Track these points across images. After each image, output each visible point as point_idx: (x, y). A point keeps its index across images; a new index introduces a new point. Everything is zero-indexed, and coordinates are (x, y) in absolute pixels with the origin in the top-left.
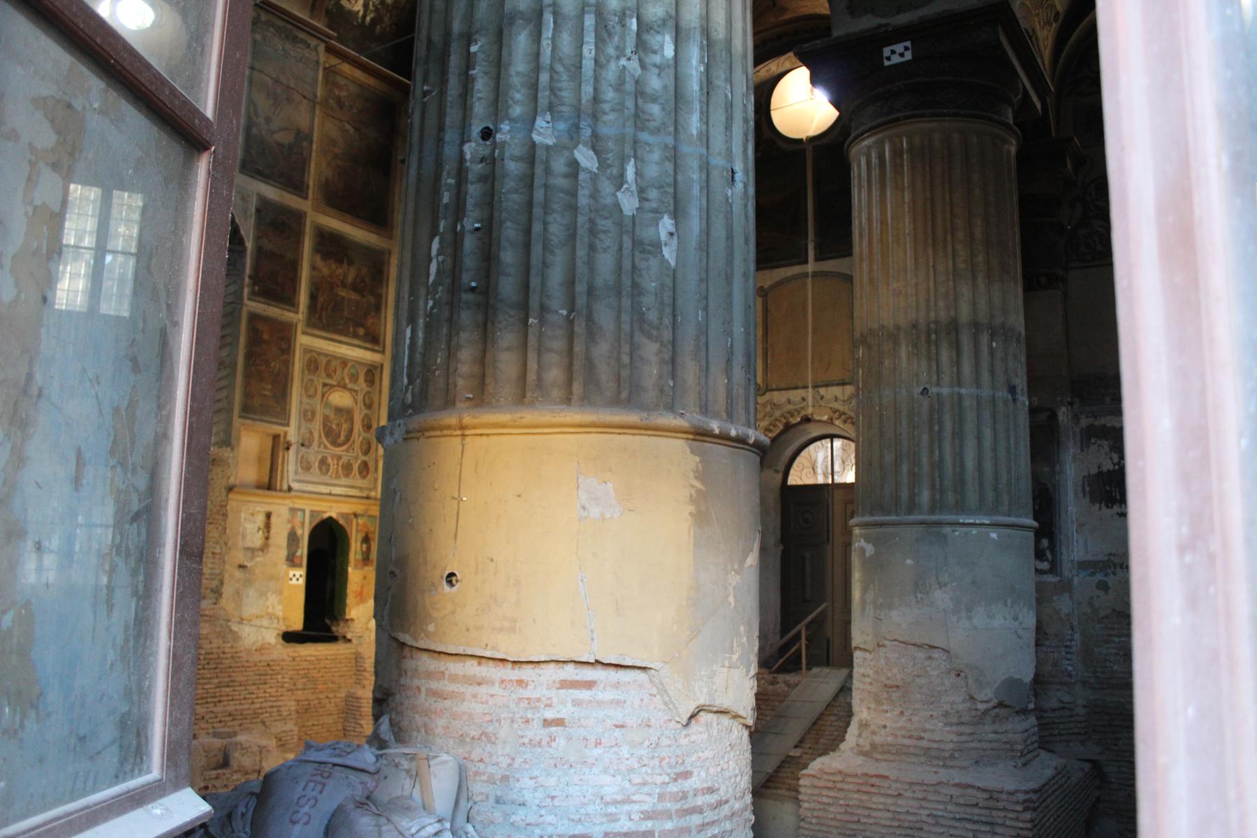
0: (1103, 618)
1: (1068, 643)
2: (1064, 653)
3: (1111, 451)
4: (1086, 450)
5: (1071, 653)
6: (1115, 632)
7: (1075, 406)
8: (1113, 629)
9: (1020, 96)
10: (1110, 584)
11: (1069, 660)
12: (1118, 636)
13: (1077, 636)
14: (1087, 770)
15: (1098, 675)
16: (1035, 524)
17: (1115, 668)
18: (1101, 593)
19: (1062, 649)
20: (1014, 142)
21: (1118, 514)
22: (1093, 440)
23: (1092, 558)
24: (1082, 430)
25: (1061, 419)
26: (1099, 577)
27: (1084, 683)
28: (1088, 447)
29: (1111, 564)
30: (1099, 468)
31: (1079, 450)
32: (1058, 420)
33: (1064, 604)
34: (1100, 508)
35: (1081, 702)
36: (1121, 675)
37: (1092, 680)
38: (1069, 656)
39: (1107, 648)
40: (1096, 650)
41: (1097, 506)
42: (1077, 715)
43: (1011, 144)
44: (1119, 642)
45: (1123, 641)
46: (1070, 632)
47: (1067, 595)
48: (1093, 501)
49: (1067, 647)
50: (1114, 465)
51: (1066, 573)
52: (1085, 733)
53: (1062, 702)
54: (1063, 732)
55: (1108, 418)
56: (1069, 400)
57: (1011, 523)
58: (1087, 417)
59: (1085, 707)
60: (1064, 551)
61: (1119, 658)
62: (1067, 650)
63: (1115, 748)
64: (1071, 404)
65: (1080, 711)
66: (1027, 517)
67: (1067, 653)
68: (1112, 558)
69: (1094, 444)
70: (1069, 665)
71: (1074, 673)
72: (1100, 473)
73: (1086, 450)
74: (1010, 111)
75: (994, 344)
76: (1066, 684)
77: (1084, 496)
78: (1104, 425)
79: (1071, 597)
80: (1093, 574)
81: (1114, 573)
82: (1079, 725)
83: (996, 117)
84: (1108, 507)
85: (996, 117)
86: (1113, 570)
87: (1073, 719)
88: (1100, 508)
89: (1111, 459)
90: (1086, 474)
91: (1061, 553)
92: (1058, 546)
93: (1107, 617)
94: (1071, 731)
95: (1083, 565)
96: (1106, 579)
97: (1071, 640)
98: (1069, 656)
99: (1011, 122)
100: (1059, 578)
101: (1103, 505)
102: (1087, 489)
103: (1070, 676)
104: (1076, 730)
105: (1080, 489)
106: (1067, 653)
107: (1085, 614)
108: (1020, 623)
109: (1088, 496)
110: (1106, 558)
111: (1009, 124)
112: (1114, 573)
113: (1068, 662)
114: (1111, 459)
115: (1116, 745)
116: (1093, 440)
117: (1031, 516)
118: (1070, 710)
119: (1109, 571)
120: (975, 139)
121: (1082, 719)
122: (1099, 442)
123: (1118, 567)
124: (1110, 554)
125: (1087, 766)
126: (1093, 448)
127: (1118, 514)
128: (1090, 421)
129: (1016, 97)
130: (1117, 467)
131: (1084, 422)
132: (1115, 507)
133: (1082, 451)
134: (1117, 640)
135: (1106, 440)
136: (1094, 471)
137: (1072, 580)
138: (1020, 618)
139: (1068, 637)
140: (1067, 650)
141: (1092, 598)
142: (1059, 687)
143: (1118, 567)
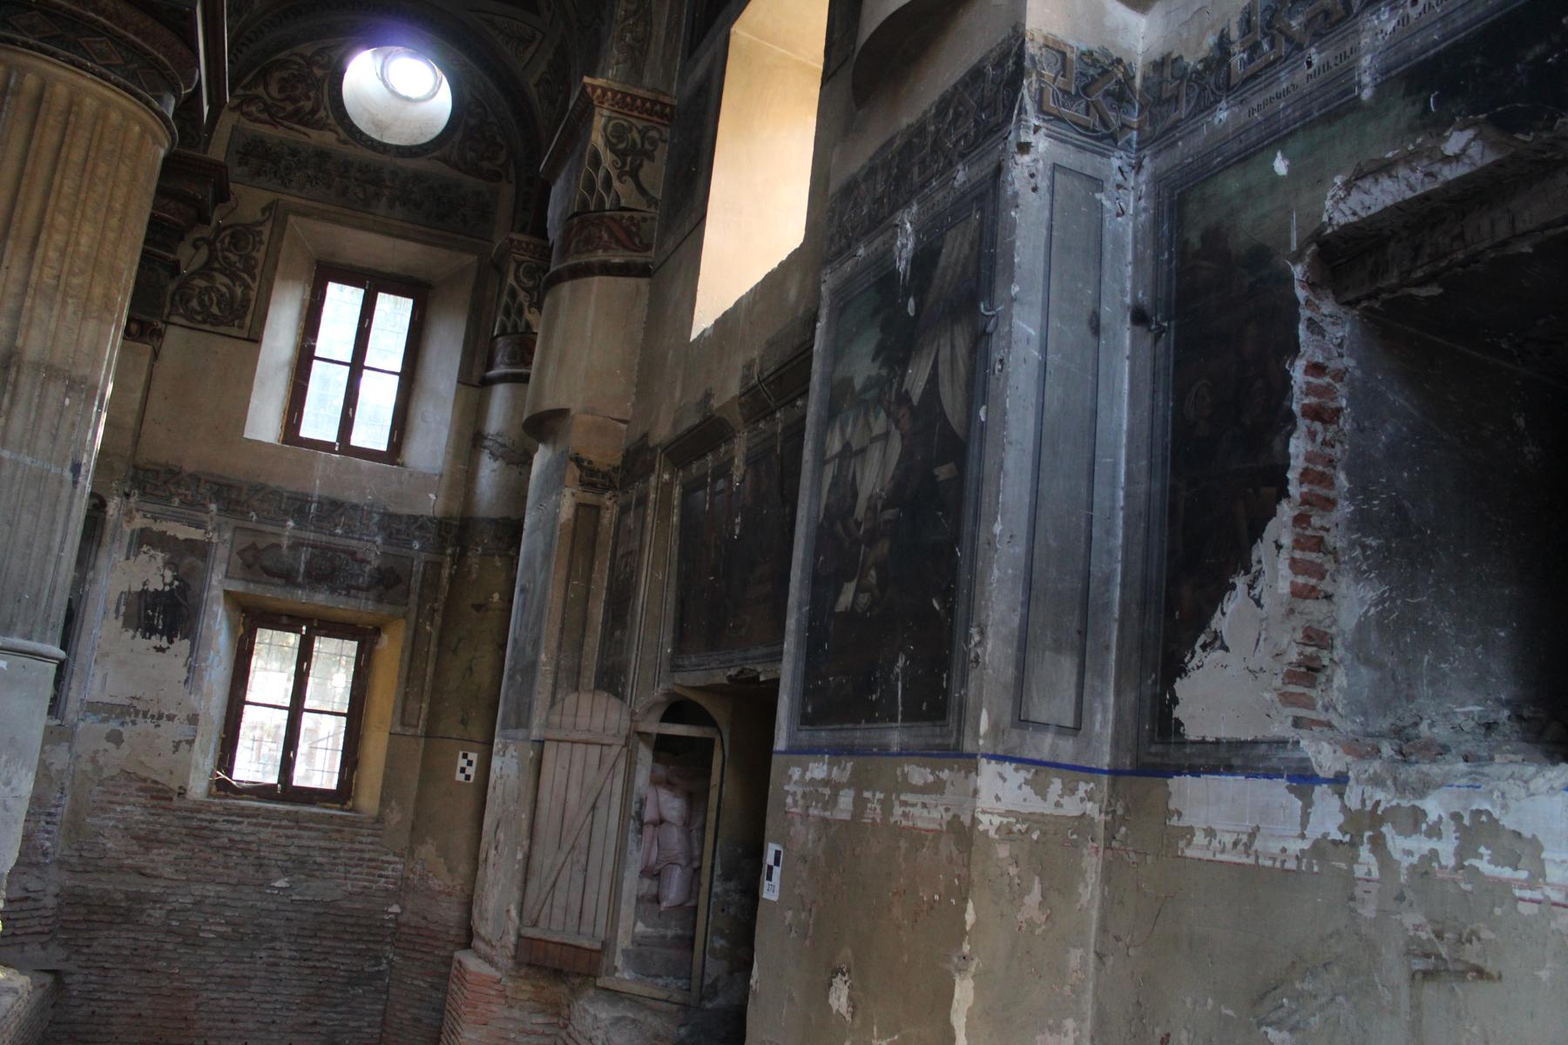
0: (107, 779)
1: (53, 810)
2: (43, 823)
3: (164, 567)
4: (132, 558)
5: (54, 824)
6: (118, 799)
7: (132, 500)
8: (117, 794)
9: (190, 90)
10: (125, 736)
11: (48, 832)
12: (120, 804)
13: (66, 801)
14: (48, 986)
15: (84, 854)
16: (62, 654)
17: (109, 845)
18: (110, 746)
19: (43, 817)
20: (167, 145)
21: (155, 647)
22: (145, 548)
23: (106, 699)
24: (133, 532)
25: (111, 512)
26: (113, 725)
27: (61, 864)
28: (136, 556)
29: (132, 710)
30: (144, 584)
31: (123, 558)
32: (105, 513)
33: (60, 758)
34: (134, 637)
35: (53, 889)
36: (113, 854)
37: (73, 860)
38: (49, 827)
39: (105, 819)
40: (88, 820)
41: (131, 633)
42: (45, 907)
43: (162, 146)
44: (122, 812)
45: (127, 811)
46: (58, 795)
47: (65, 745)
48: (126, 625)
49: (50, 814)
50: (165, 585)
51: (71, 716)
52: (51, 931)
53: (27, 890)
54: (18, 932)
55: (172, 524)
56: (127, 490)
57: (31, 650)
58: (145, 516)
59: (57, 896)
60: (74, 685)
61: (116, 832)
62: (49, 819)
63: (86, 950)
64: (127, 495)
65: (50, 902)
66: (53, 644)
67: (48, 823)
68: (135, 703)
69: (145, 553)
70: (48, 839)
71: (51, 850)
72: (144, 592)
73: (132, 558)
74: (173, 102)
75: (67, 401)
76: (37, 865)
77: (116, 618)
78: (164, 533)
79: (70, 748)
80: (105, 720)
81: (134, 723)
82: (43, 922)
83: (156, 104)
84: (144, 637)
85: (156, 104)
86: (133, 717)
87: (38, 913)
88: (134, 637)
89: (163, 576)
90: (126, 590)
91: (70, 689)
92: (67, 679)
93: (112, 778)
94: (30, 930)
95: (93, 707)
96: (121, 729)
97: (58, 806)
98: (49, 827)
99: (170, 116)
100: (58, 722)
101: (138, 634)
102: (123, 609)
103: (45, 854)
104: (39, 929)
105: (113, 607)
106: (48, 823)
107: (83, 772)
108: (12, 790)
109: (121, 619)
110: (127, 702)
111: (167, 117)
112: (134, 723)
113: (46, 836)
114: (163, 576)
115: (88, 946)
116: (145, 548)
117: (58, 641)
118: (35, 900)
119: (128, 719)
120: (137, 129)
121: (50, 913)
122: (152, 552)
123: (141, 715)
124: (133, 698)
125: (48, 979)
126: (142, 557)
127: (155, 647)
128: (147, 523)
129: (187, 87)
130: (167, 588)
131: (139, 522)
132: (153, 638)
133: (128, 558)
134: (119, 809)
135: (162, 552)
136: (137, 587)
137: (76, 725)
138: (14, 782)
139: (53, 802)
140: (49, 819)
141: (96, 752)
142: (26, 869)
143: (141, 715)
